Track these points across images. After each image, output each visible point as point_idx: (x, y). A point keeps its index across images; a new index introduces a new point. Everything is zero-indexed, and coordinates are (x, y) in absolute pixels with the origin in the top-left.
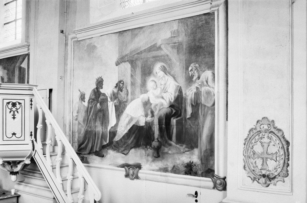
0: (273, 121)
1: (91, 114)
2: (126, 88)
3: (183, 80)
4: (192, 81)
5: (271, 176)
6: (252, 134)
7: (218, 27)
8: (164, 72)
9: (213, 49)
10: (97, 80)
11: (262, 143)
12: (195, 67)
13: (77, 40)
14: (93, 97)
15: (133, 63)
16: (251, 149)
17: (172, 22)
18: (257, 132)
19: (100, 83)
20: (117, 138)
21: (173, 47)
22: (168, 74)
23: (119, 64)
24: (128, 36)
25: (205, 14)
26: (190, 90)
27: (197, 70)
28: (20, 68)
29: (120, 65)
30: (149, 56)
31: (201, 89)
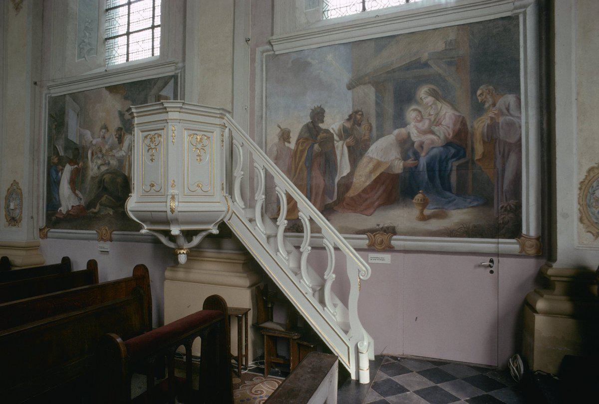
1: (303, 159)
2: (368, 121)
4: (483, 109)
6: (592, 174)
7: (525, 36)
8: (434, 97)
13: (274, 54)
14: (307, 135)
15: (378, 85)
19: (318, 115)
20: (351, 193)
21: (450, 64)
23: (354, 87)
25: (502, 18)
26: (479, 121)
27: (490, 94)
29: (355, 89)
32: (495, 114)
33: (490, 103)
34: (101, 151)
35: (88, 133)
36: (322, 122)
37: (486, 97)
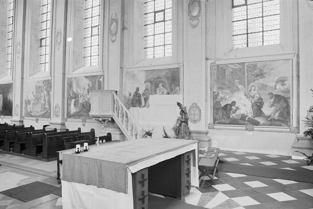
0: (197, 104)
5: (196, 120)
15: (151, 82)
19: (138, 89)
21: (166, 78)
23: (146, 83)
25: (177, 68)
28: (99, 81)
34: (83, 96)
35: (79, 90)
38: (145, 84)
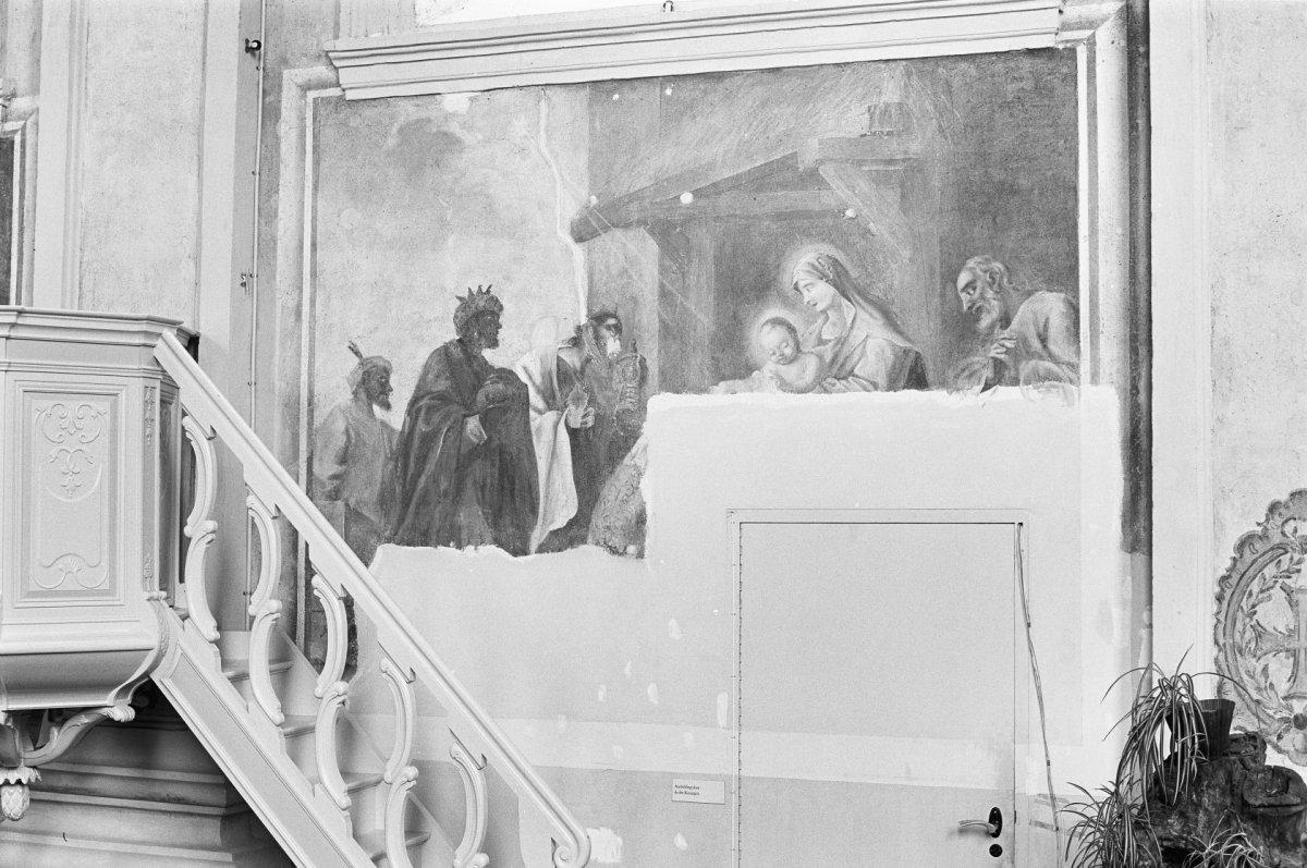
3: (931, 324)
4: (975, 332)
6: (1248, 557)
7: (1093, 113)
8: (836, 286)
9: (1070, 204)
10: (465, 303)
11: (1289, 592)
12: (985, 272)
13: (341, 98)
14: (442, 385)
15: (670, 233)
16: (1248, 619)
17: (873, 65)
18: (1272, 549)
19: (480, 318)
21: (880, 180)
22: (858, 298)
23: (594, 234)
24: (643, 110)
25: (1031, 52)
27: (995, 287)
29: (597, 242)
30: (757, 210)
31: (1017, 370)
32: (1008, 351)
33: (995, 314)
36: (494, 343)
37: (982, 297)
38: (578, 251)
